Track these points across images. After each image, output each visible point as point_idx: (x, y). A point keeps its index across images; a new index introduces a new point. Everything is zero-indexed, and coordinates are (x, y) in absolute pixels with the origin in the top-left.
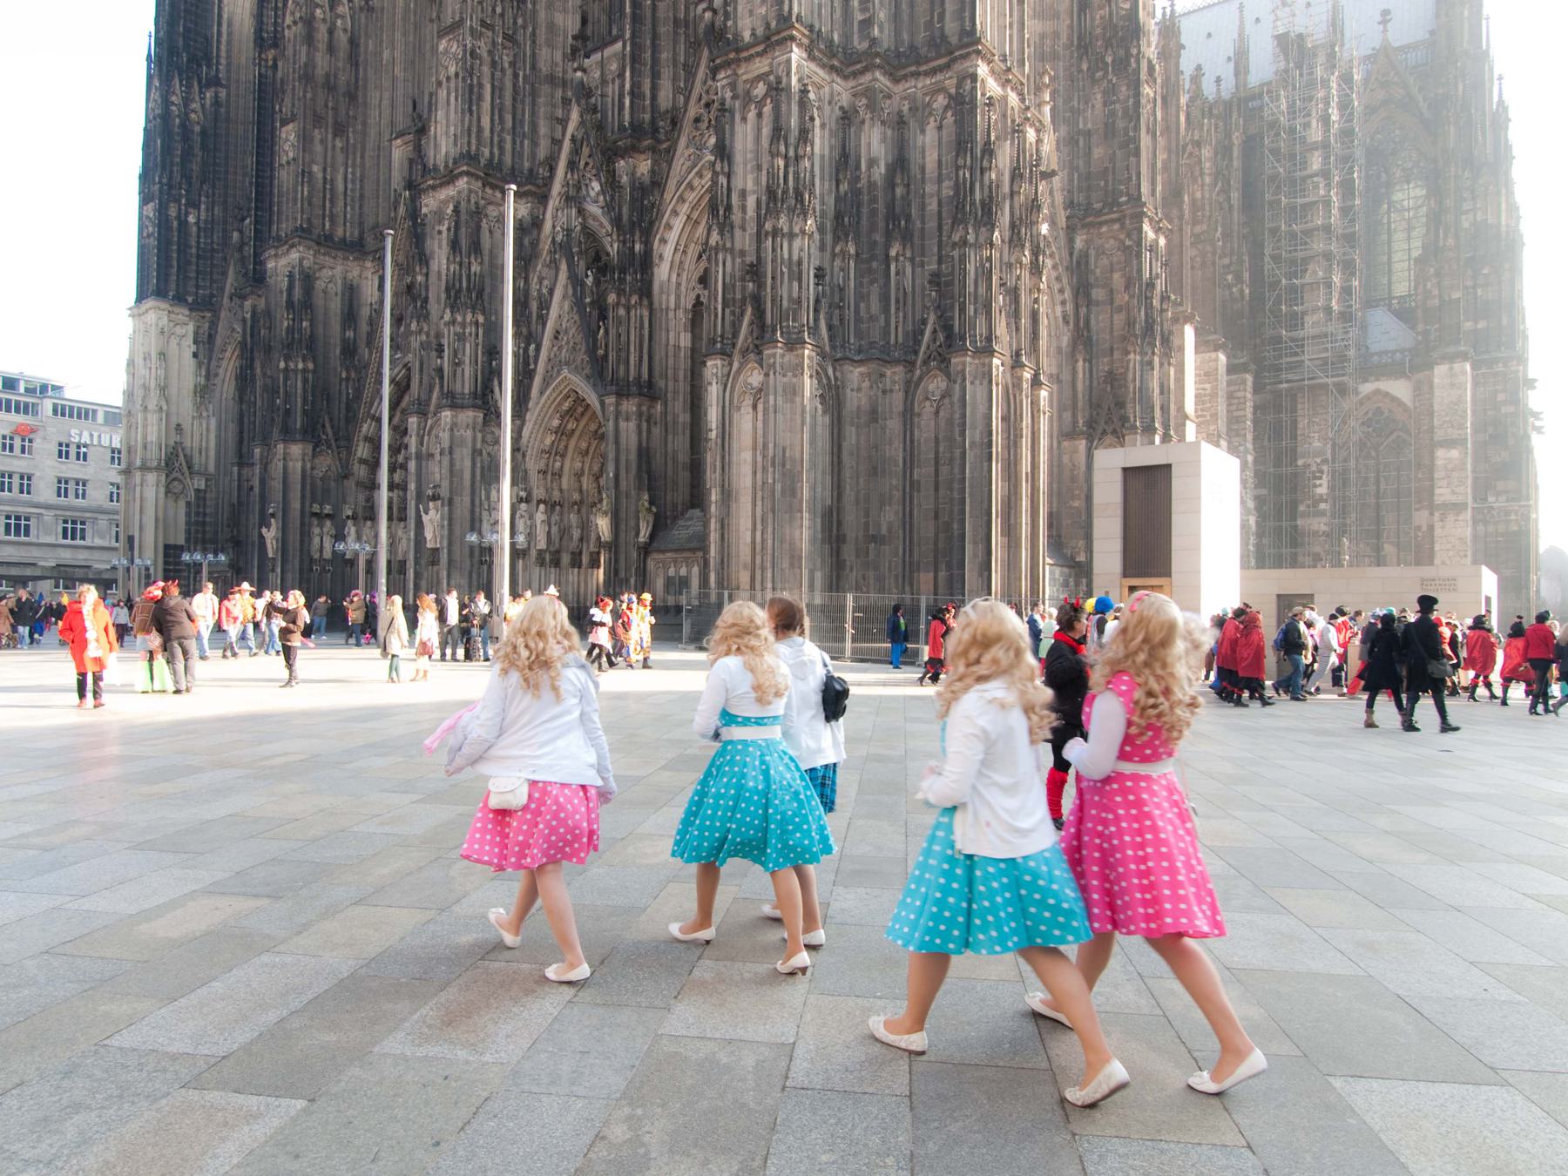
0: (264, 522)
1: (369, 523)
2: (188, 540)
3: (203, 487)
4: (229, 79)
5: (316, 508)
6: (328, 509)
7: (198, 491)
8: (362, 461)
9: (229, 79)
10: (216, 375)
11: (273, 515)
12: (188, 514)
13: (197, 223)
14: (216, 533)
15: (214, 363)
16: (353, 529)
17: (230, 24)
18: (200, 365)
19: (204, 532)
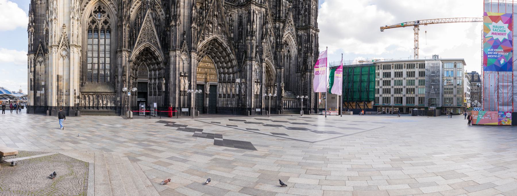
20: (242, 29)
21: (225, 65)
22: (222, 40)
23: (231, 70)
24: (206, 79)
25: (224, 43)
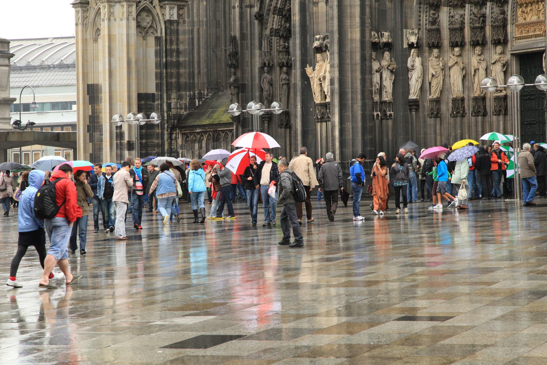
0: (307, 60)
1: (436, 51)
2: (159, 87)
3: (175, 18)
5: (374, 37)
6: (386, 37)
7: (169, 23)
11: (319, 50)
12: (158, 54)
14: (192, 75)
16: (418, 61)
19: (178, 75)
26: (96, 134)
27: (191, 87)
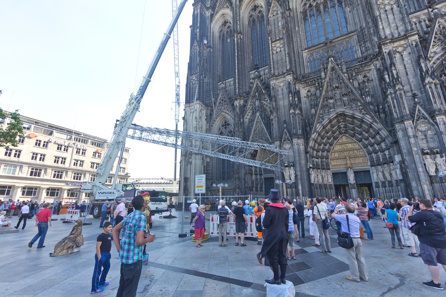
4: (213, 47)
7: (207, 162)
8: (311, 147)
9: (213, 47)
10: (212, 126)
13: (206, 82)
14: (212, 176)
15: (212, 122)
17: (213, 33)
18: (207, 122)
20: (385, 84)
21: (373, 141)
22: (352, 112)
23: (383, 145)
24: (346, 164)
25: (356, 114)
26: (186, 191)
27: (212, 179)
